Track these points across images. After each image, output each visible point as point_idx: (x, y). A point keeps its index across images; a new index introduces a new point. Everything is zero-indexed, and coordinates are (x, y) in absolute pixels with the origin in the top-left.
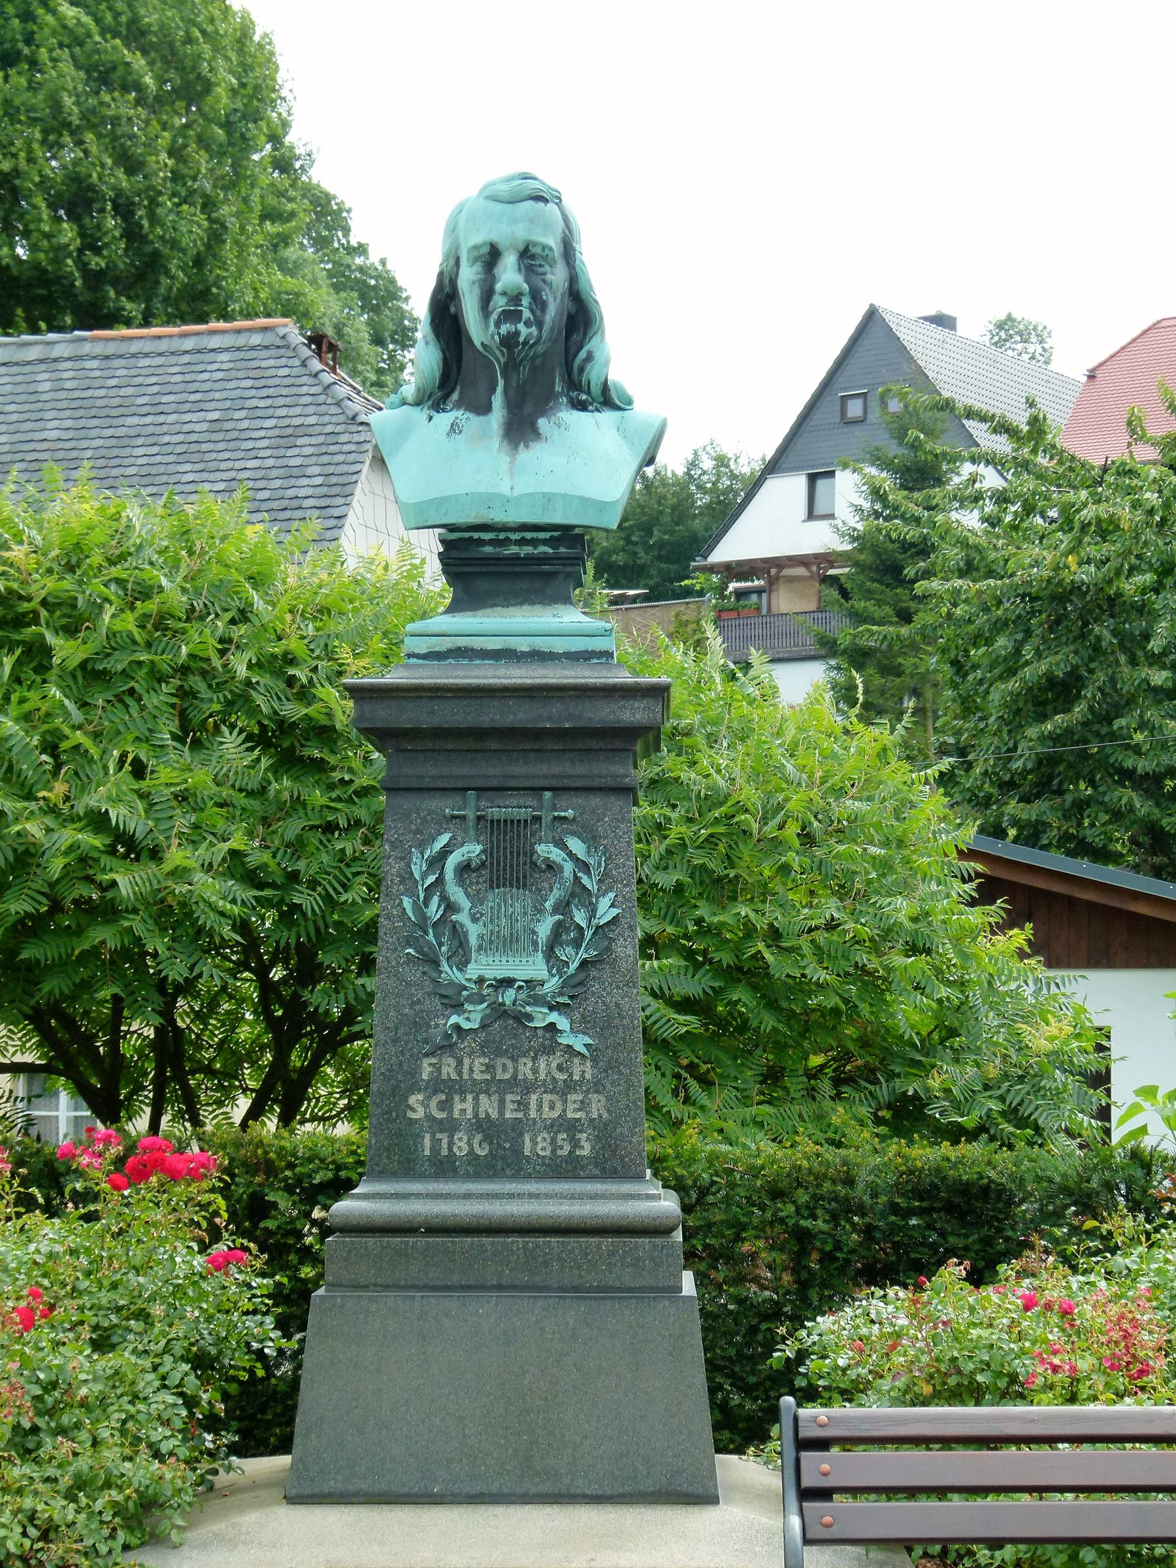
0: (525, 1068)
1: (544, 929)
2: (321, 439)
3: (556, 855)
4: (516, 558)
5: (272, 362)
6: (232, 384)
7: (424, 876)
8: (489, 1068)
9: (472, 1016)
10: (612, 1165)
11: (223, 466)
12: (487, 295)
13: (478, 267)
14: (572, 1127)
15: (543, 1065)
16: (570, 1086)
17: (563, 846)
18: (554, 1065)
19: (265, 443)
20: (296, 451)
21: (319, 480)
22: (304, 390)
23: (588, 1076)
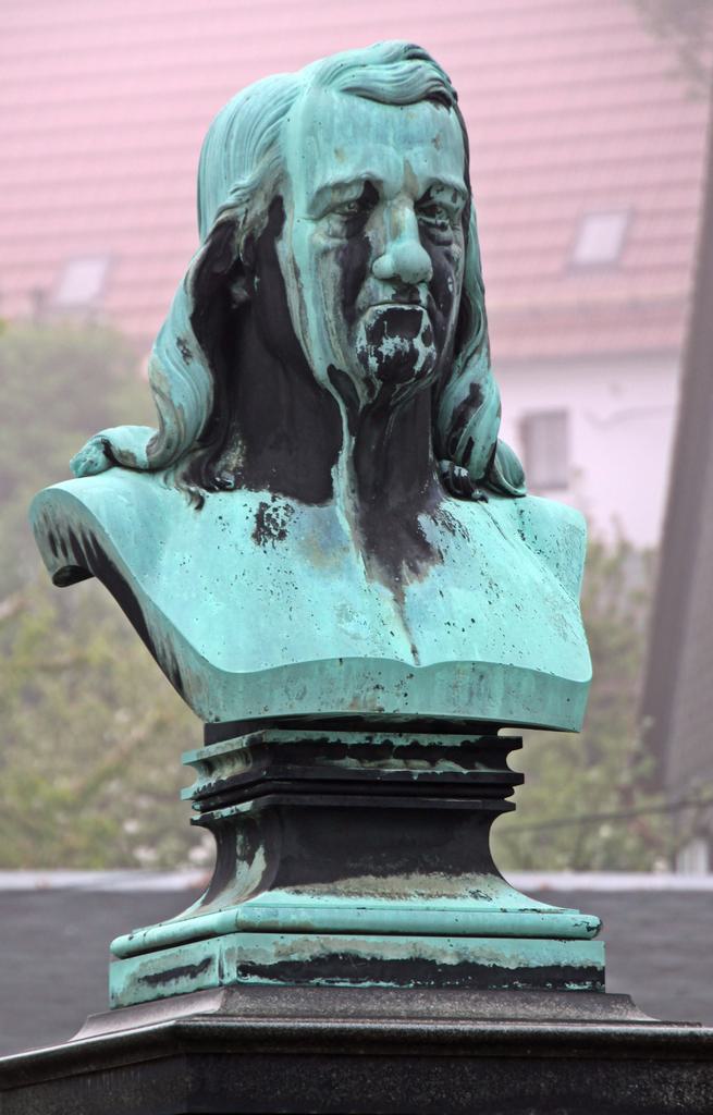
4: (403, 784)
13: (335, 223)
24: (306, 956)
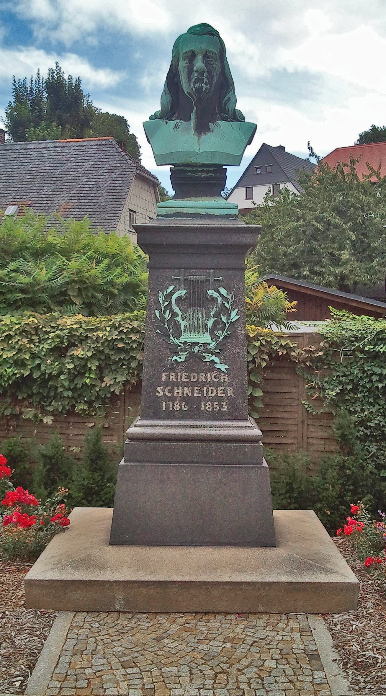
0: (202, 377)
1: (210, 323)
2: (121, 170)
3: (215, 294)
4: (200, 177)
5: (108, 149)
6: (97, 155)
7: (164, 302)
8: (188, 377)
9: (182, 357)
10: (234, 415)
11: (94, 177)
12: (190, 72)
14: (220, 400)
15: (209, 376)
16: (219, 384)
17: (218, 292)
18: (213, 376)
19: (106, 171)
20: (114, 173)
21: (121, 182)
22: (117, 156)
23: (226, 380)
24: (172, 213)
